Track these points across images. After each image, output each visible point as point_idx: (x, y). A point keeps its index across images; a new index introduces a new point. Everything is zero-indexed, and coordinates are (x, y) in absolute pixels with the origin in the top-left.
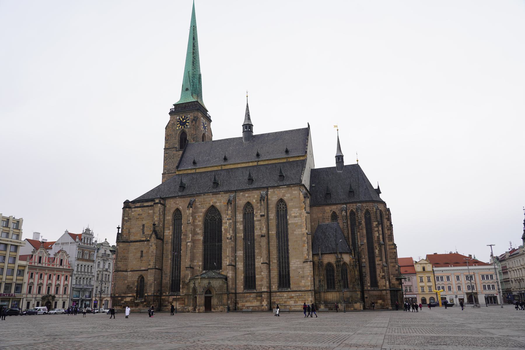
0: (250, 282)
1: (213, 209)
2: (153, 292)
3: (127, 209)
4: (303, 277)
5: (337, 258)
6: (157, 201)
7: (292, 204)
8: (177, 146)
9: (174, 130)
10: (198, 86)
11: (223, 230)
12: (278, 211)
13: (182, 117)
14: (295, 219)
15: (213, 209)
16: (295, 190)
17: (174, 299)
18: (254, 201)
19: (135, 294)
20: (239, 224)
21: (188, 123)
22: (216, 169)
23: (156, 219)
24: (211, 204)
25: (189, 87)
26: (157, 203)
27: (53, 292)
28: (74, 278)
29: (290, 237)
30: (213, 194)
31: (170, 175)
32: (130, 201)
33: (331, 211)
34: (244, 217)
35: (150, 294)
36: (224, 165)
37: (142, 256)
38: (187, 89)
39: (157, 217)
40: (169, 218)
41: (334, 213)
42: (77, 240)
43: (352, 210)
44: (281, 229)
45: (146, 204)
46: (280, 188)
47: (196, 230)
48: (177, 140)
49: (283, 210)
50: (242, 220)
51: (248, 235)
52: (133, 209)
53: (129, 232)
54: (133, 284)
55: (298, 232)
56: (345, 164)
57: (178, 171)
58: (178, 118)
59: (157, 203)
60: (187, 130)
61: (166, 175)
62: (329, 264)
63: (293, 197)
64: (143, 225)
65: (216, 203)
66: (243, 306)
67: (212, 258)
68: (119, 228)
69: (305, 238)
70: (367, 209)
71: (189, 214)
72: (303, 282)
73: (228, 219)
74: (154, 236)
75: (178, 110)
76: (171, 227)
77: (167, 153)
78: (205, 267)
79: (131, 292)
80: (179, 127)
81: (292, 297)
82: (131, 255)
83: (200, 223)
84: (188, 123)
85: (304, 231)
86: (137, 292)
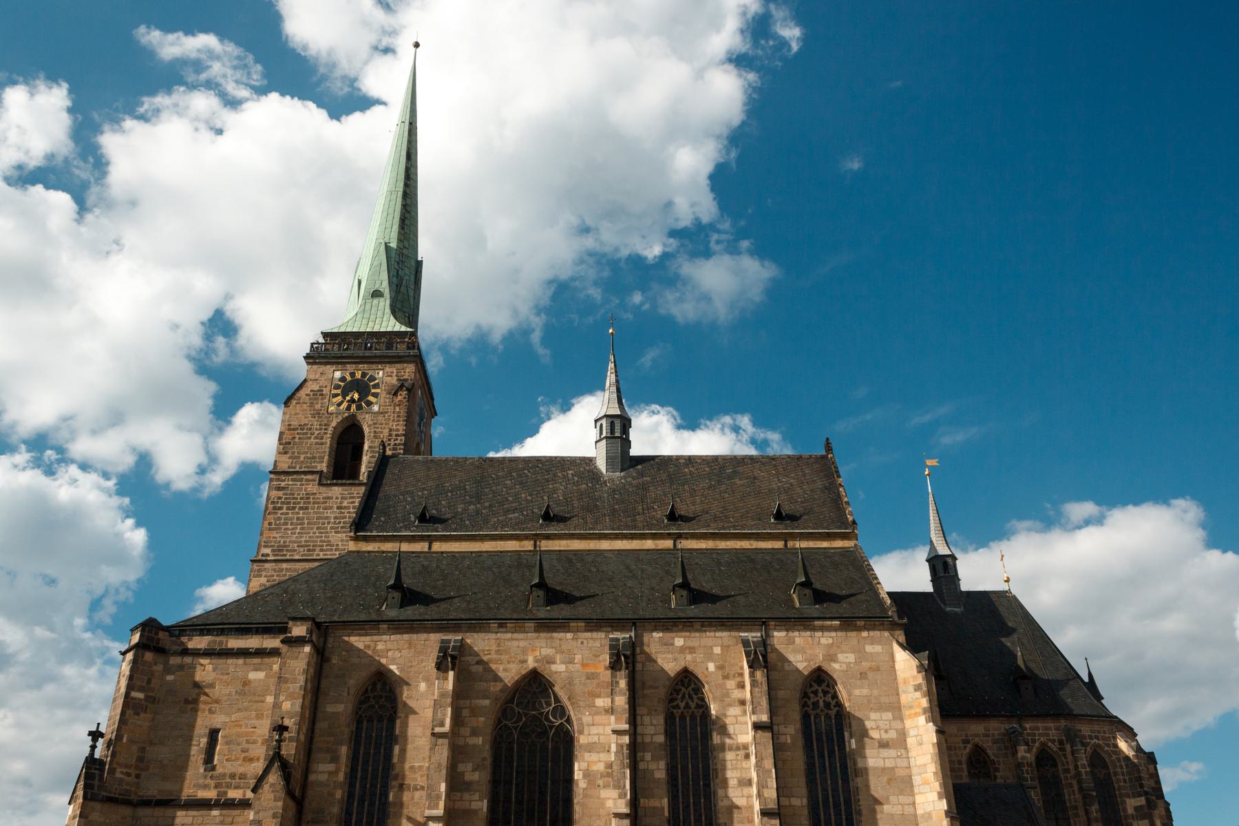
3: (149, 656)
6: (299, 630)
7: (865, 691)
8: (323, 466)
9: (317, 414)
10: (411, 293)
11: (578, 775)
12: (805, 717)
13: (353, 375)
14: (885, 752)
16: (873, 642)
18: (711, 667)
20: (648, 756)
21: (375, 395)
22: (512, 545)
23: (287, 706)
24: (531, 664)
25: (385, 287)
26: (300, 641)
30: (538, 629)
31: (284, 565)
32: (166, 621)
33: (966, 742)
34: (669, 733)
36: (548, 537)
38: (376, 294)
39: (291, 696)
40: (339, 708)
41: (978, 751)
43: (1043, 744)
44: (825, 790)
45: (235, 643)
46: (814, 629)
47: (461, 768)
48: (326, 448)
49: (828, 717)
50: (661, 739)
51: (687, 807)
53: (141, 759)
56: (965, 586)
57: (356, 539)
58: (338, 374)
59: (300, 641)
61: (267, 565)
63: (866, 665)
65: (551, 661)
68: (95, 735)
70: (1099, 746)
71: (443, 695)
73: (614, 732)
74: (274, 778)
76: (344, 750)
77: (279, 489)
83: (479, 741)
84: (375, 395)
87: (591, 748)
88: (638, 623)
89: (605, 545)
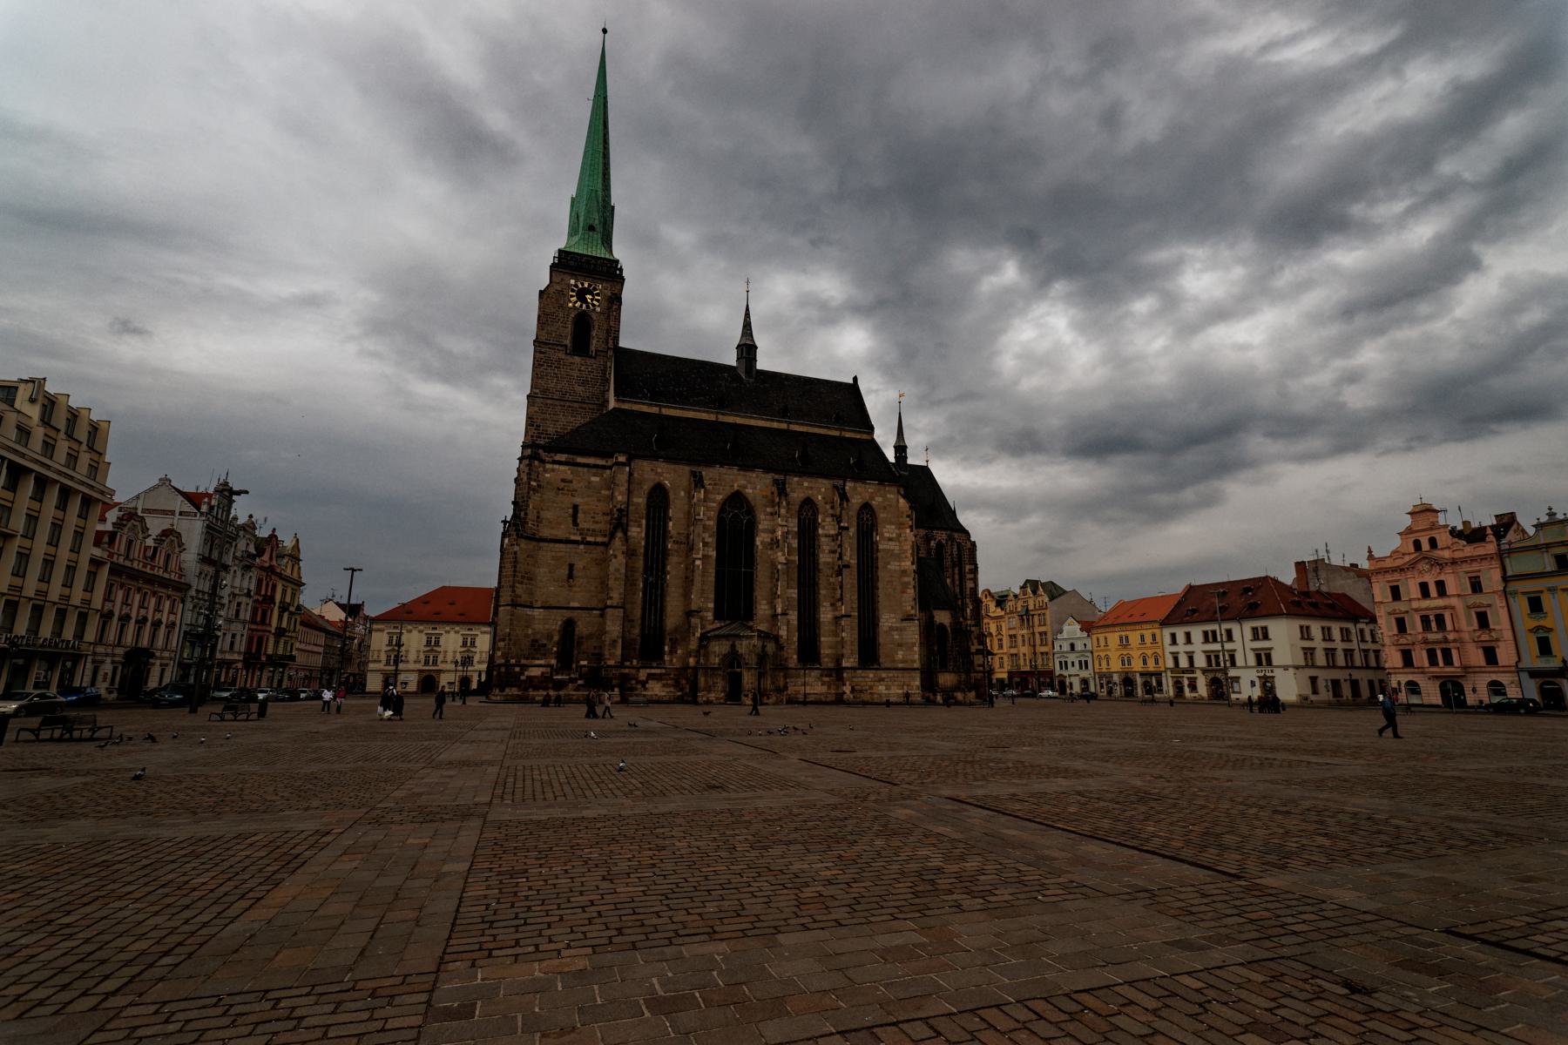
0: (809, 651)
1: (737, 499)
2: (619, 659)
4: (900, 645)
5: (954, 617)
8: (568, 342)
15: (737, 499)
17: (650, 676)
19: (553, 662)
27: (145, 643)
28: (189, 605)
29: (881, 574)
35: (611, 662)
37: (570, 576)
38: (591, 228)
40: (640, 500)
42: (204, 508)
45: (580, 460)
52: (549, 466)
54: (550, 637)
55: (893, 566)
60: (594, 316)
62: (942, 625)
64: (575, 507)
66: (798, 692)
67: (735, 597)
69: (909, 579)
72: (900, 655)
75: (565, 263)
78: (718, 615)
79: (544, 656)
80: (573, 302)
81: (882, 680)
82: (542, 572)
85: (908, 564)
86: (559, 656)
87: (765, 531)
88: (786, 472)
89: (753, 422)
